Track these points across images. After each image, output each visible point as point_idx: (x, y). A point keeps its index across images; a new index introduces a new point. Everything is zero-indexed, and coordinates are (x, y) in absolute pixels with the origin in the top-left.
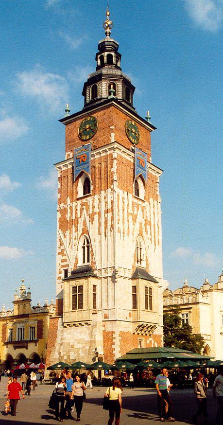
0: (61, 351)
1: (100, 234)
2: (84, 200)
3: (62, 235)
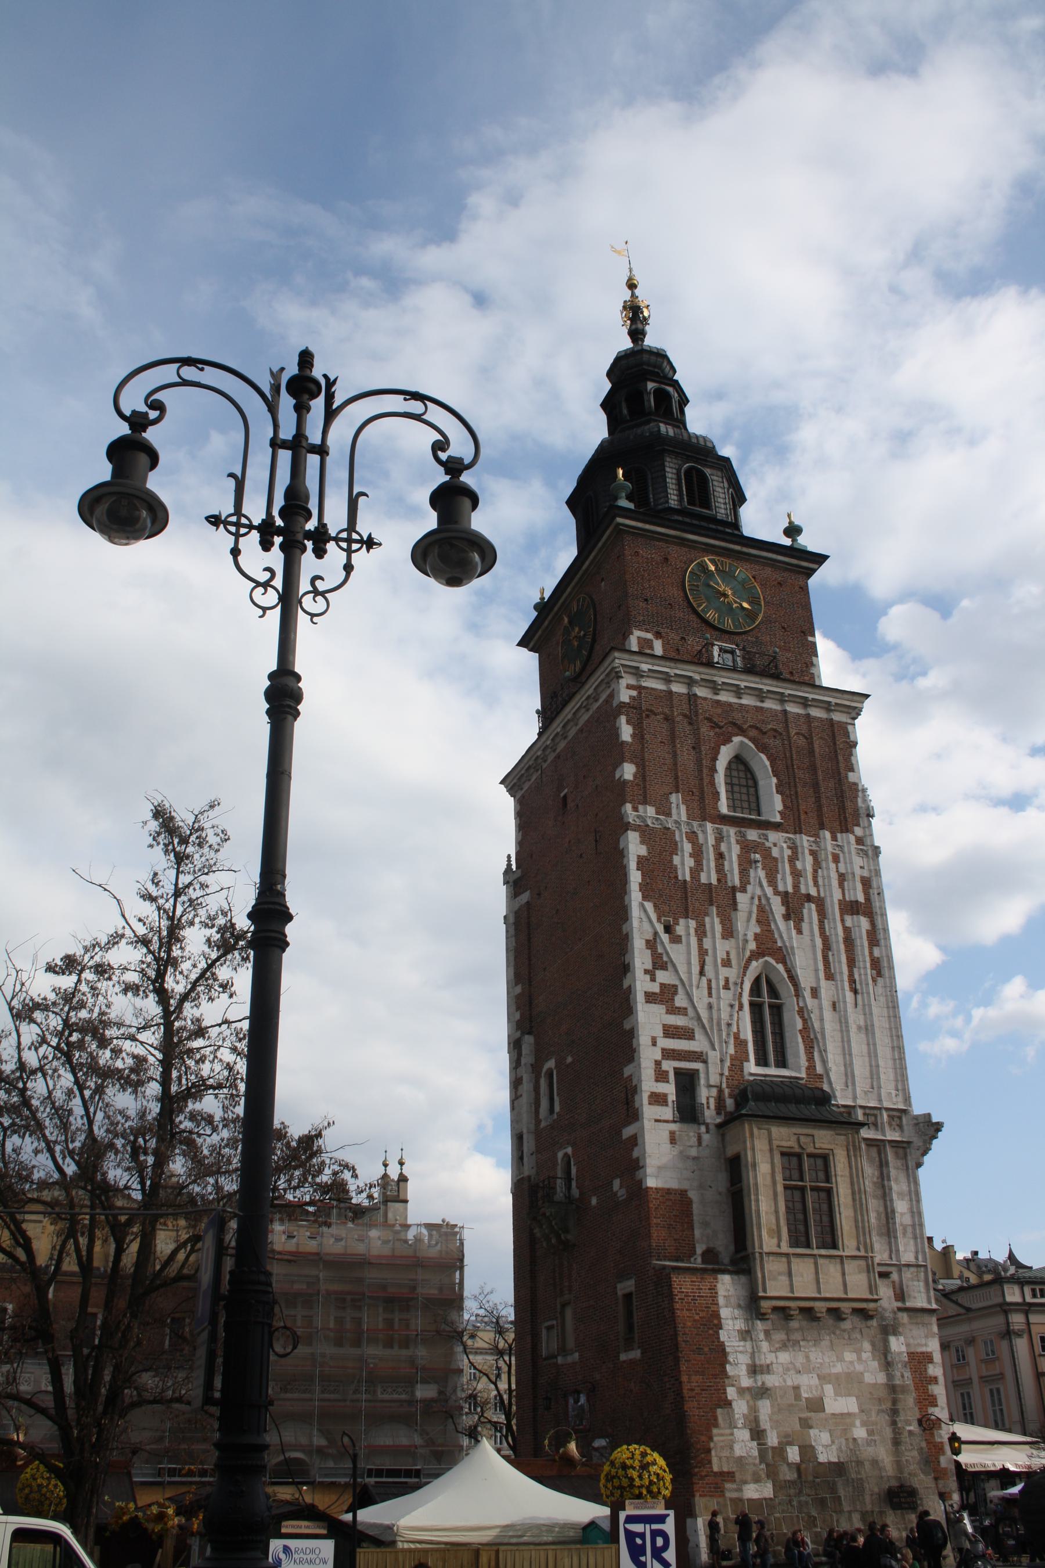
0: (765, 1424)
1: (830, 976)
2: (752, 835)
3: (660, 928)
